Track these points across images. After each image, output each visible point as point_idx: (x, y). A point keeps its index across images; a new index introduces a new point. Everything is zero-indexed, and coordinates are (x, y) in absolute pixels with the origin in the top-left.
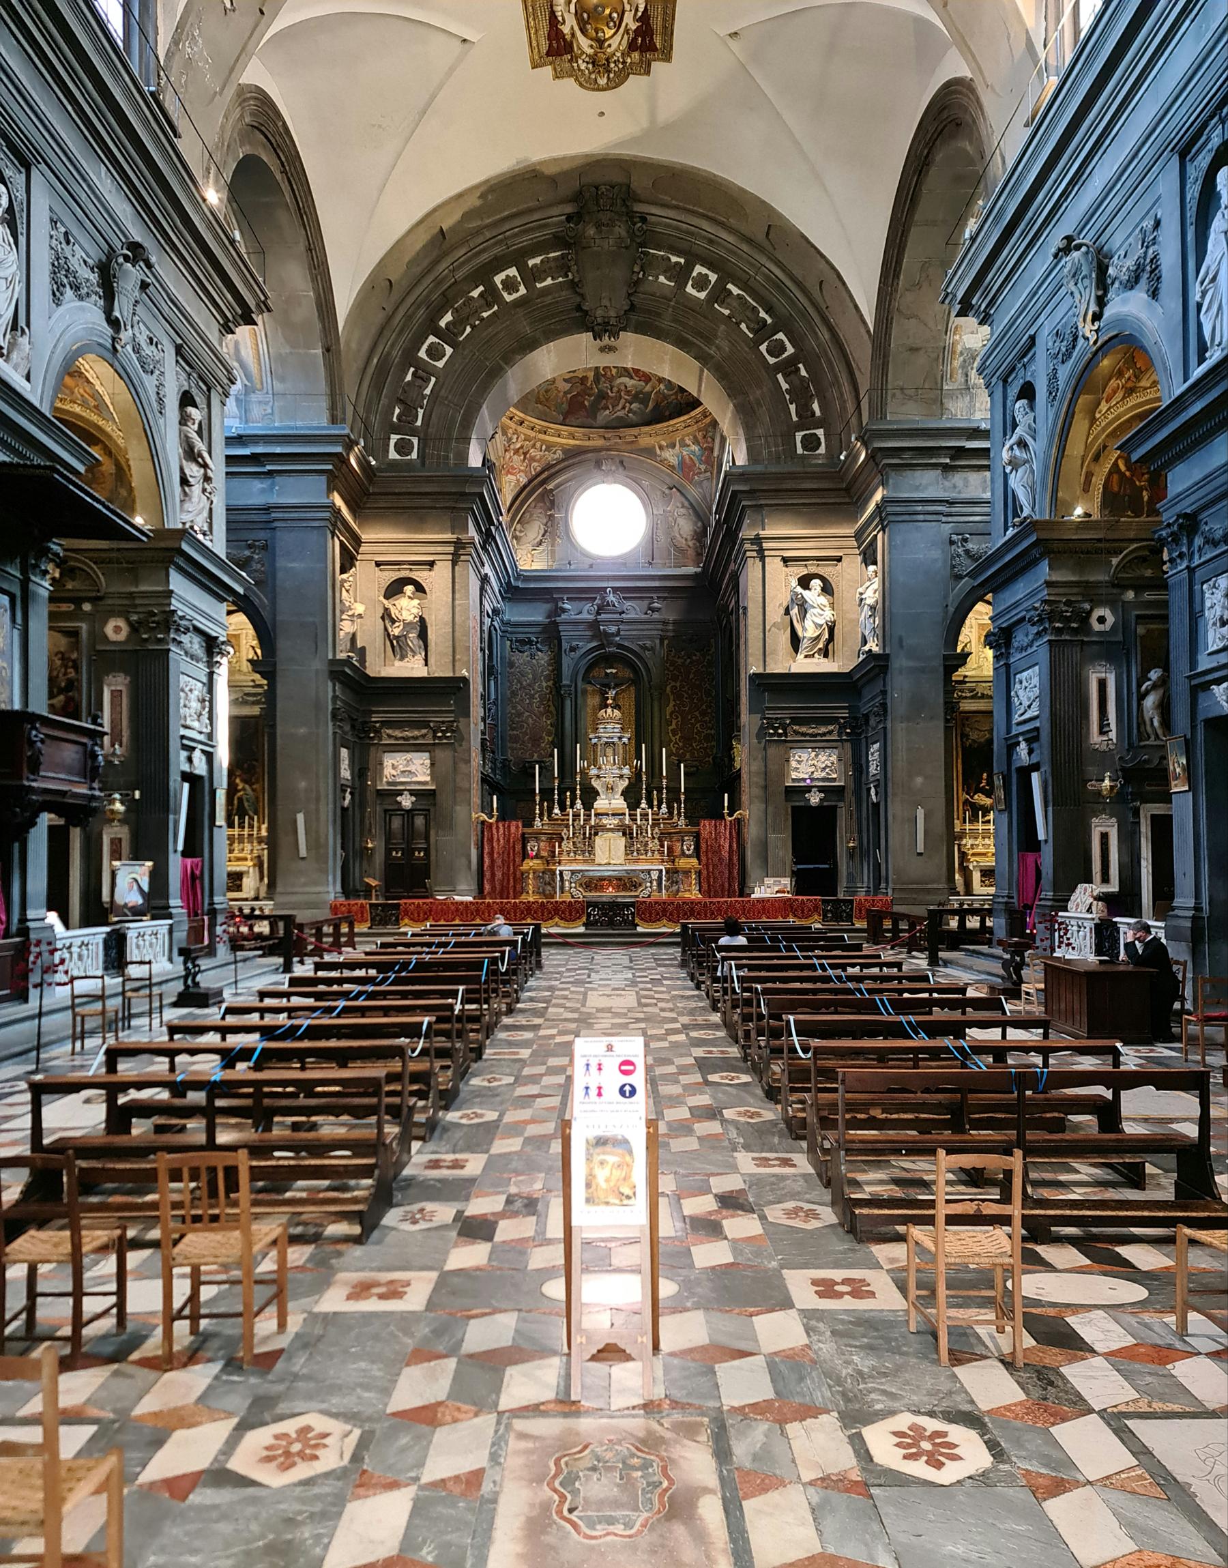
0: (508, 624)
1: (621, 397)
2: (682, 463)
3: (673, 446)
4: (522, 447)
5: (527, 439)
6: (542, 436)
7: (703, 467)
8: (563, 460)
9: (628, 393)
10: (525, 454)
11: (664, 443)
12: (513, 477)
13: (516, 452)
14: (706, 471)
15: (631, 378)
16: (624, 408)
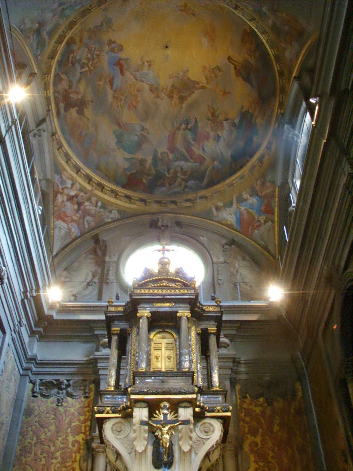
0: (33, 359)
1: (177, 177)
2: (240, 220)
3: (230, 204)
4: (76, 196)
5: (82, 189)
6: (99, 193)
7: (262, 219)
8: (119, 220)
9: (184, 173)
10: (79, 204)
11: (221, 204)
12: (64, 225)
13: (71, 198)
14: (266, 222)
15: (187, 160)
16: (180, 185)
